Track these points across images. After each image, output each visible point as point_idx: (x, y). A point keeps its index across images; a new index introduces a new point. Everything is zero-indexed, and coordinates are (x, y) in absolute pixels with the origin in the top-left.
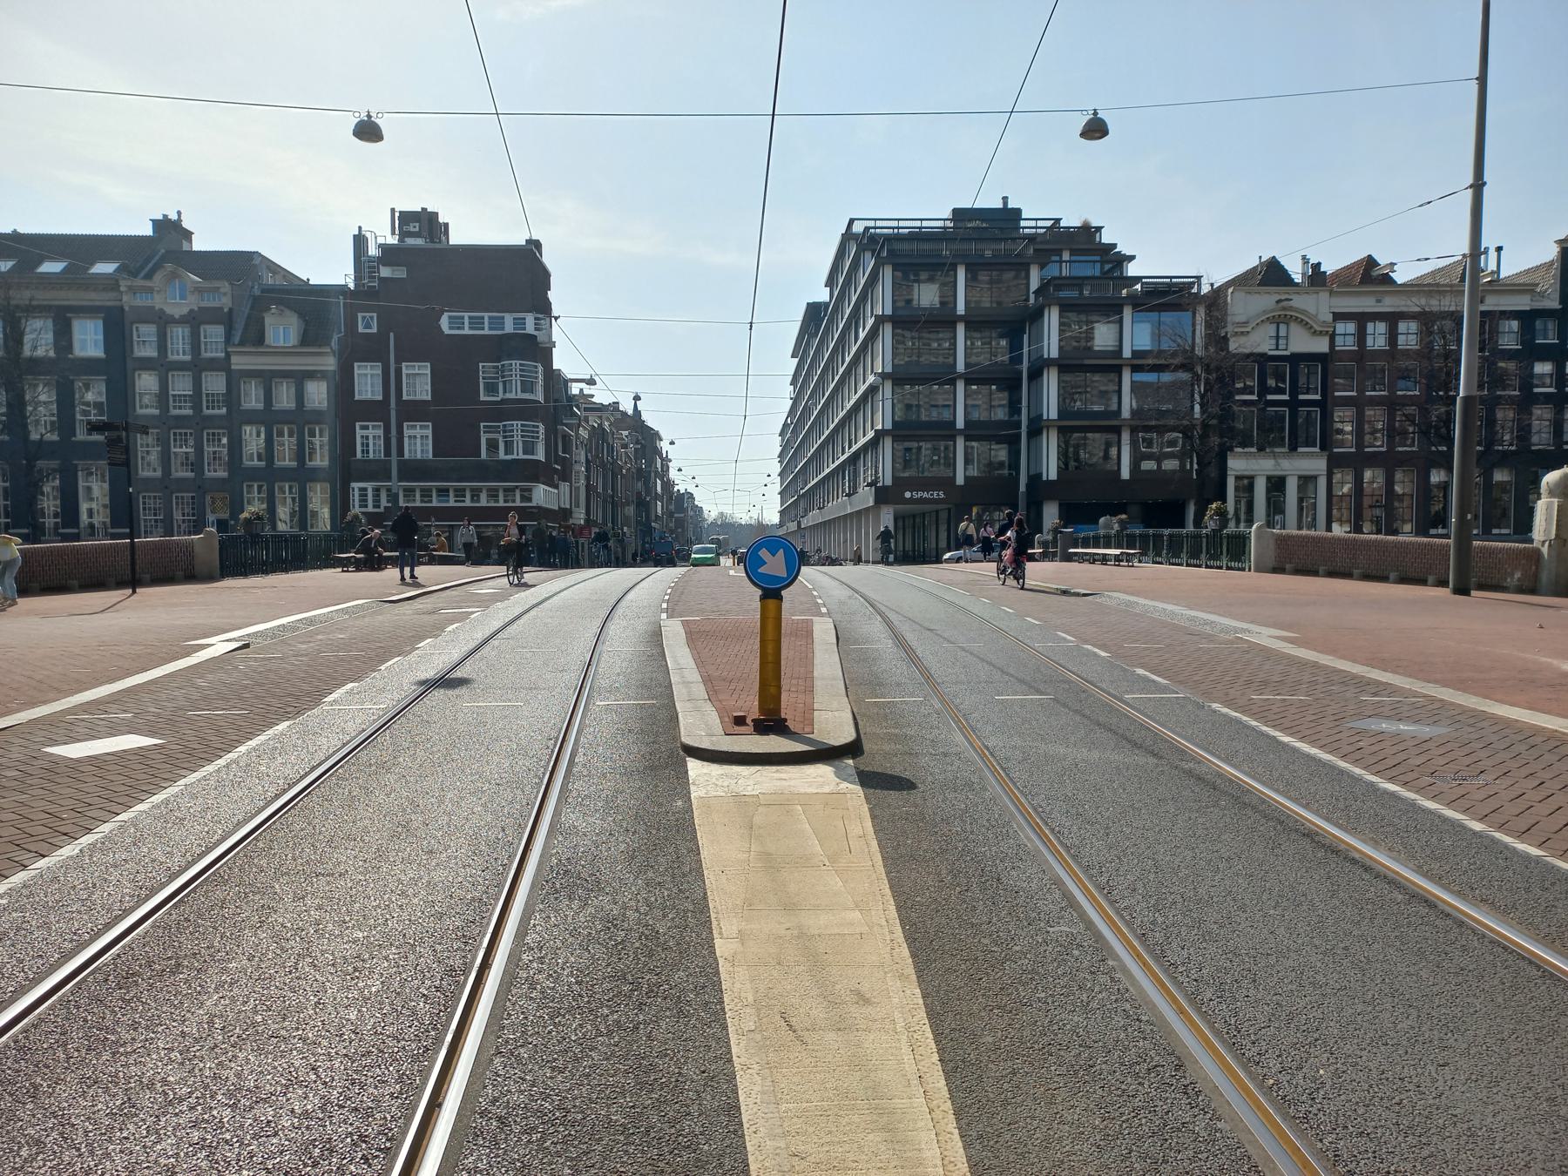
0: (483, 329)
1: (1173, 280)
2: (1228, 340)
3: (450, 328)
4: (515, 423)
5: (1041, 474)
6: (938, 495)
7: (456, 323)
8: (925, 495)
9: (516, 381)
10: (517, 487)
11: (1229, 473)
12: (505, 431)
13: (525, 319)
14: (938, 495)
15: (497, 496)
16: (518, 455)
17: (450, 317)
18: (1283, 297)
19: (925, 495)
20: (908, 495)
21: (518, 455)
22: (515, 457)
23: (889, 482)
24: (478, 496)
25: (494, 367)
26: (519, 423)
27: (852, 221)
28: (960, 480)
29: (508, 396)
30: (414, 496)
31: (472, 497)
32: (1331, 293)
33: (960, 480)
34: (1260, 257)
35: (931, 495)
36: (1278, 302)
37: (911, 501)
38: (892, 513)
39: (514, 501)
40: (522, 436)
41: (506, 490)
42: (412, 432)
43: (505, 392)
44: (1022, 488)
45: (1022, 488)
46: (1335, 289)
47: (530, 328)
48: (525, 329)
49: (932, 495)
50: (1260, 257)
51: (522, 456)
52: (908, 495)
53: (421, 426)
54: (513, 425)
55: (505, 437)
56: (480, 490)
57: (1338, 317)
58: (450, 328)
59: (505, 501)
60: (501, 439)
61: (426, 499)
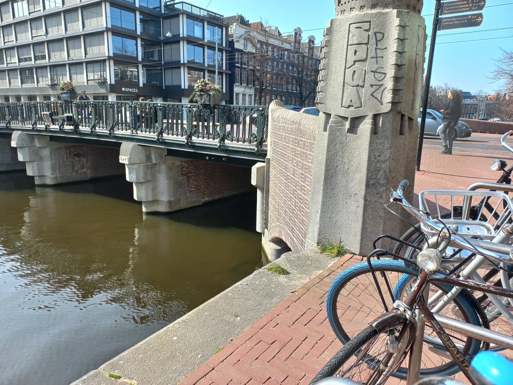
1: (217, 15)
5: (180, 86)
6: (135, 91)
8: (130, 90)
14: (135, 91)
18: (247, 31)
19: (130, 90)
20: (123, 89)
23: (113, 82)
28: (141, 85)
33: (141, 85)
34: (237, 14)
37: (125, 92)
38: (115, 97)
46: (258, 31)
49: (133, 90)
50: (237, 14)
52: (123, 89)
57: (259, 41)
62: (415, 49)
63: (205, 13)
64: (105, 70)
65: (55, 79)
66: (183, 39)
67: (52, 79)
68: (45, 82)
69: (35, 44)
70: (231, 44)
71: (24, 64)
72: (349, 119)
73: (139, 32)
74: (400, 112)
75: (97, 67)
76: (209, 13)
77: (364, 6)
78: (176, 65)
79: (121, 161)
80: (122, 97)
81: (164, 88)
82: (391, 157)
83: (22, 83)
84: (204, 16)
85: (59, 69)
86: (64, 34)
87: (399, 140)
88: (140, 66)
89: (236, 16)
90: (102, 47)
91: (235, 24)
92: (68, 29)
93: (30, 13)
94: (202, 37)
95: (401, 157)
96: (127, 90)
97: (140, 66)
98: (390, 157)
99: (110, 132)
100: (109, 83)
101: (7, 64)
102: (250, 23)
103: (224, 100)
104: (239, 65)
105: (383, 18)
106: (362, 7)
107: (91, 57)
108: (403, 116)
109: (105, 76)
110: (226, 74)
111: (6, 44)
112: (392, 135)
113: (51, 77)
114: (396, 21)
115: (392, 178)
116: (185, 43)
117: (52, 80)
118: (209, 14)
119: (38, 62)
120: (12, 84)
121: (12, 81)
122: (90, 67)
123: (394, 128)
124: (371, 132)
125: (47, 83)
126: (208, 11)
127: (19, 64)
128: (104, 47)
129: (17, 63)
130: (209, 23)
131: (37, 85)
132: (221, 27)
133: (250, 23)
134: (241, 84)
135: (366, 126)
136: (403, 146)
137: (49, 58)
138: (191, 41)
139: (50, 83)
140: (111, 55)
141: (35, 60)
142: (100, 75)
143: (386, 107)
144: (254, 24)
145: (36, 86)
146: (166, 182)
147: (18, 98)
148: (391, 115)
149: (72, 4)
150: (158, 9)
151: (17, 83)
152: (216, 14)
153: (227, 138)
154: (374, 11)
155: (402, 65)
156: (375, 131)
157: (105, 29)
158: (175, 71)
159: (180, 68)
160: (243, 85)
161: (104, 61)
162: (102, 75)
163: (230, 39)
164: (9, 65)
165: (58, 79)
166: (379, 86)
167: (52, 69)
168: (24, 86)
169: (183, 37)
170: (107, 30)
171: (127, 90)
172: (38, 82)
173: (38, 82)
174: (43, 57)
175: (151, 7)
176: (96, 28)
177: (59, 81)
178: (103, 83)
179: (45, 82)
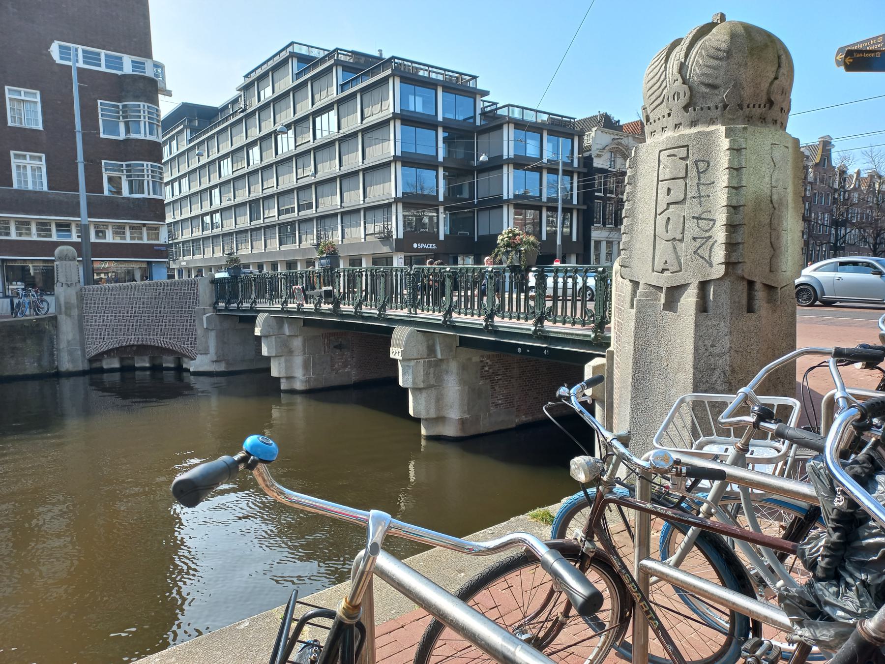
0: (100, 65)
1: (564, 118)
2: (592, 159)
3: (61, 58)
4: (145, 163)
6: (432, 247)
7: (64, 51)
9: (145, 122)
10: (144, 225)
11: (592, 238)
12: (127, 171)
13: (144, 64)
14: (432, 247)
15: (124, 233)
16: (149, 194)
17: (60, 47)
18: (616, 137)
19: (425, 246)
20: (415, 245)
21: (149, 194)
22: (145, 195)
23: (401, 236)
24: (103, 232)
25: (114, 106)
26: (150, 163)
27: (292, 44)
28: (442, 238)
29: (133, 136)
30: (29, 229)
31: (97, 233)
32: (634, 137)
33: (442, 238)
34: (599, 112)
35: (429, 246)
36: (614, 139)
37: (417, 250)
38: (403, 258)
39: (141, 239)
40: (153, 177)
41: (132, 227)
42: (21, 162)
43: (128, 131)
44: (559, 242)
45: (559, 242)
46: (636, 136)
47: (149, 72)
48: (145, 73)
49: (429, 246)
50: (599, 112)
51: (152, 196)
52: (415, 245)
53: (31, 157)
54: (143, 165)
55: (128, 176)
56: (106, 225)
58: (61, 58)
59: (132, 238)
60: (124, 178)
61: (43, 233)
62: (767, 179)
63: (545, 117)
64: (389, 219)
65: (322, 236)
66: (509, 161)
67: (318, 237)
68: (309, 241)
69: (300, 189)
70: (587, 161)
71: (285, 217)
72: (664, 290)
73: (441, 159)
74: (743, 278)
75: (379, 214)
76: (551, 116)
77: (680, 124)
78: (497, 203)
79: (392, 356)
80: (413, 258)
81: (476, 240)
82: (733, 347)
83: (280, 244)
84: (543, 123)
85: (328, 222)
86: (338, 171)
87: (746, 322)
88: (441, 209)
89: (596, 116)
90: (387, 184)
91: (594, 129)
92: (344, 163)
93: (296, 147)
94: (539, 157)
95: (752, 347)
96: (421, 246)
97: (441, 209)
98: (731, 347)
99: (380, 313)
100: (394, 237)
101: (264, 219)
102: (621, 124)
103: (573, 253)
104: (601, 195)
105: (707, 139)
106: (677, 126)
107: (371, 200)
108: (751, 284)
109: (389, 227)
110: (578, 210)
111: (264, 191)
112: (732, 313)
113: (318, 234)
114: (725, 143)
115: (738, 382)
116: (511, 167)
117: (319, 237)
118: (552, 118)
119: (302, 213)
120: (268, 247)
121: (268, 242)
122: (370, 215)
123: (735, 302)
124: (696, 308)
125: (312, 242)
126: (549, 114)
127: (278, 218)
128: (390, 185)
129: (277, 216)
130: (551, 133)
131: (299, 246)
132: (570, 136)
133: (621, 124)
134: (604, 225)
135: (689, 300)
136: (755, 331)
137: (317, 207)
138: (520, 163)
139: (315, 242)
140: (400, 195)
141: (299, 211)
142: (382, 226)
143: (718, 271)
144: (628, 125)
145: (298, 247)
146: (457, 388)
147: (274, 266)
148: (727, 283)
149: (350, 128)
150: (471, 121)
151: (274, 244)
152: (562, 117)
153: (546, 319)
154: (694, 130)
155: (740, 206)
156: (703, 307)
157: (392, 159)
158: (493, 213)
159: (502, 207)
160: (607, 226)
161: (389, 205)
162: (386, 226)
163: (586, 154)
164: (266, 221)
165: (327, 236)
166: (705, 240)
167: (319, 221)
168: (283, 248)
169: (509, 159)
170: (396, 158)
171: (421, 246)
172: (300, 242)
173: (300, 242)
174: (309, 206)
175: (461, 118)
176: (380, 158)
177: (327, 238)
178: (386, 238)
179: (309, 241)
